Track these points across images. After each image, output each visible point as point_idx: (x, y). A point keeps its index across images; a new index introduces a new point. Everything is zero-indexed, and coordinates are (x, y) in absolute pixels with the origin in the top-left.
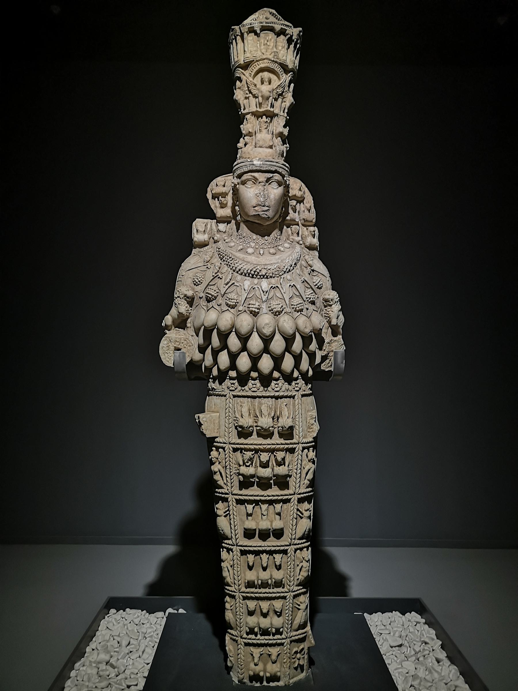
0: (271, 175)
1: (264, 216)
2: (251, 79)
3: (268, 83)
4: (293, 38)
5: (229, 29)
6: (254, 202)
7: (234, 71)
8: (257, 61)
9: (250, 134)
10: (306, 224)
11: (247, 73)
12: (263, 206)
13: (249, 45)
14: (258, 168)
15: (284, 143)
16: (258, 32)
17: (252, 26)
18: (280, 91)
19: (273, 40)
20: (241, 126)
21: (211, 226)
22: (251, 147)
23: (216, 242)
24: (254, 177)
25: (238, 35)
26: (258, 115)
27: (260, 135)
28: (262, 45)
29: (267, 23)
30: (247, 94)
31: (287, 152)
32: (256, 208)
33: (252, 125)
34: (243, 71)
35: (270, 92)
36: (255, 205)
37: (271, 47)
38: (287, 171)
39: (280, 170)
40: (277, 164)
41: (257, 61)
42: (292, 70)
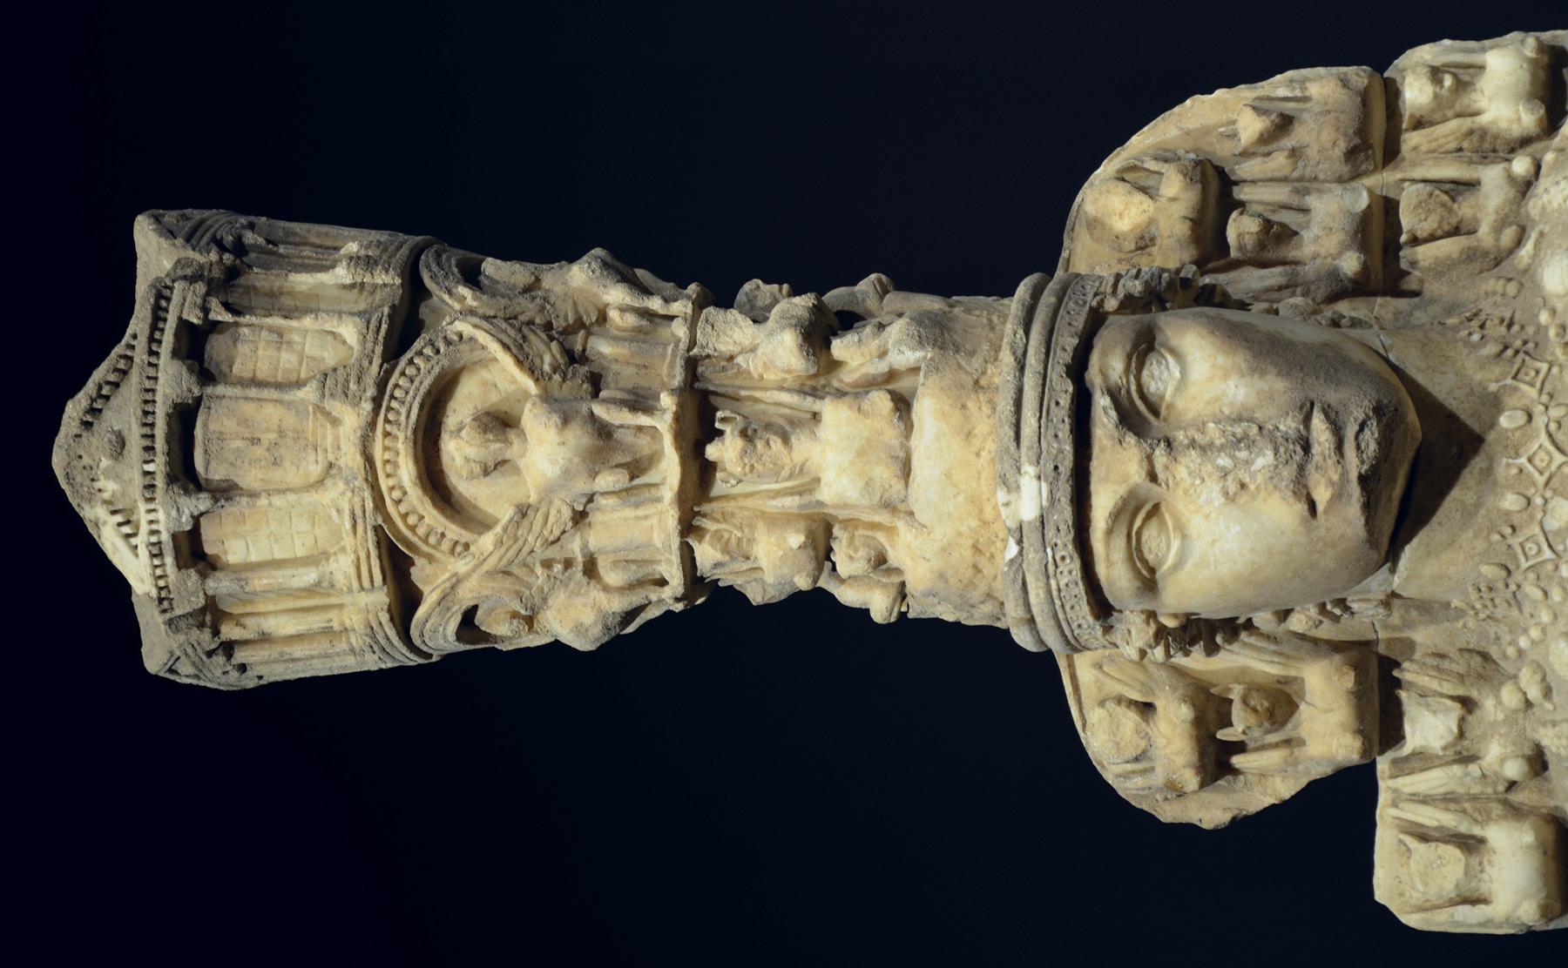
0: (1101, 402)
1: (1371, 439)
2: (487, 541)
5: (164, 687)
6: (1281, 512)
10: (1377, 135)
12: (1307, 448)
19: (248, 408)
21: (1424, 800)
23: (1538, 762)
24: (1116, 516)
27: (828, 476)
28: (276, 475)
32: (1322, 496)
35: (566, 421)
36: (1301, 507)
37: (290, 420)
39: (1067, 342)
40: (1033, 361)
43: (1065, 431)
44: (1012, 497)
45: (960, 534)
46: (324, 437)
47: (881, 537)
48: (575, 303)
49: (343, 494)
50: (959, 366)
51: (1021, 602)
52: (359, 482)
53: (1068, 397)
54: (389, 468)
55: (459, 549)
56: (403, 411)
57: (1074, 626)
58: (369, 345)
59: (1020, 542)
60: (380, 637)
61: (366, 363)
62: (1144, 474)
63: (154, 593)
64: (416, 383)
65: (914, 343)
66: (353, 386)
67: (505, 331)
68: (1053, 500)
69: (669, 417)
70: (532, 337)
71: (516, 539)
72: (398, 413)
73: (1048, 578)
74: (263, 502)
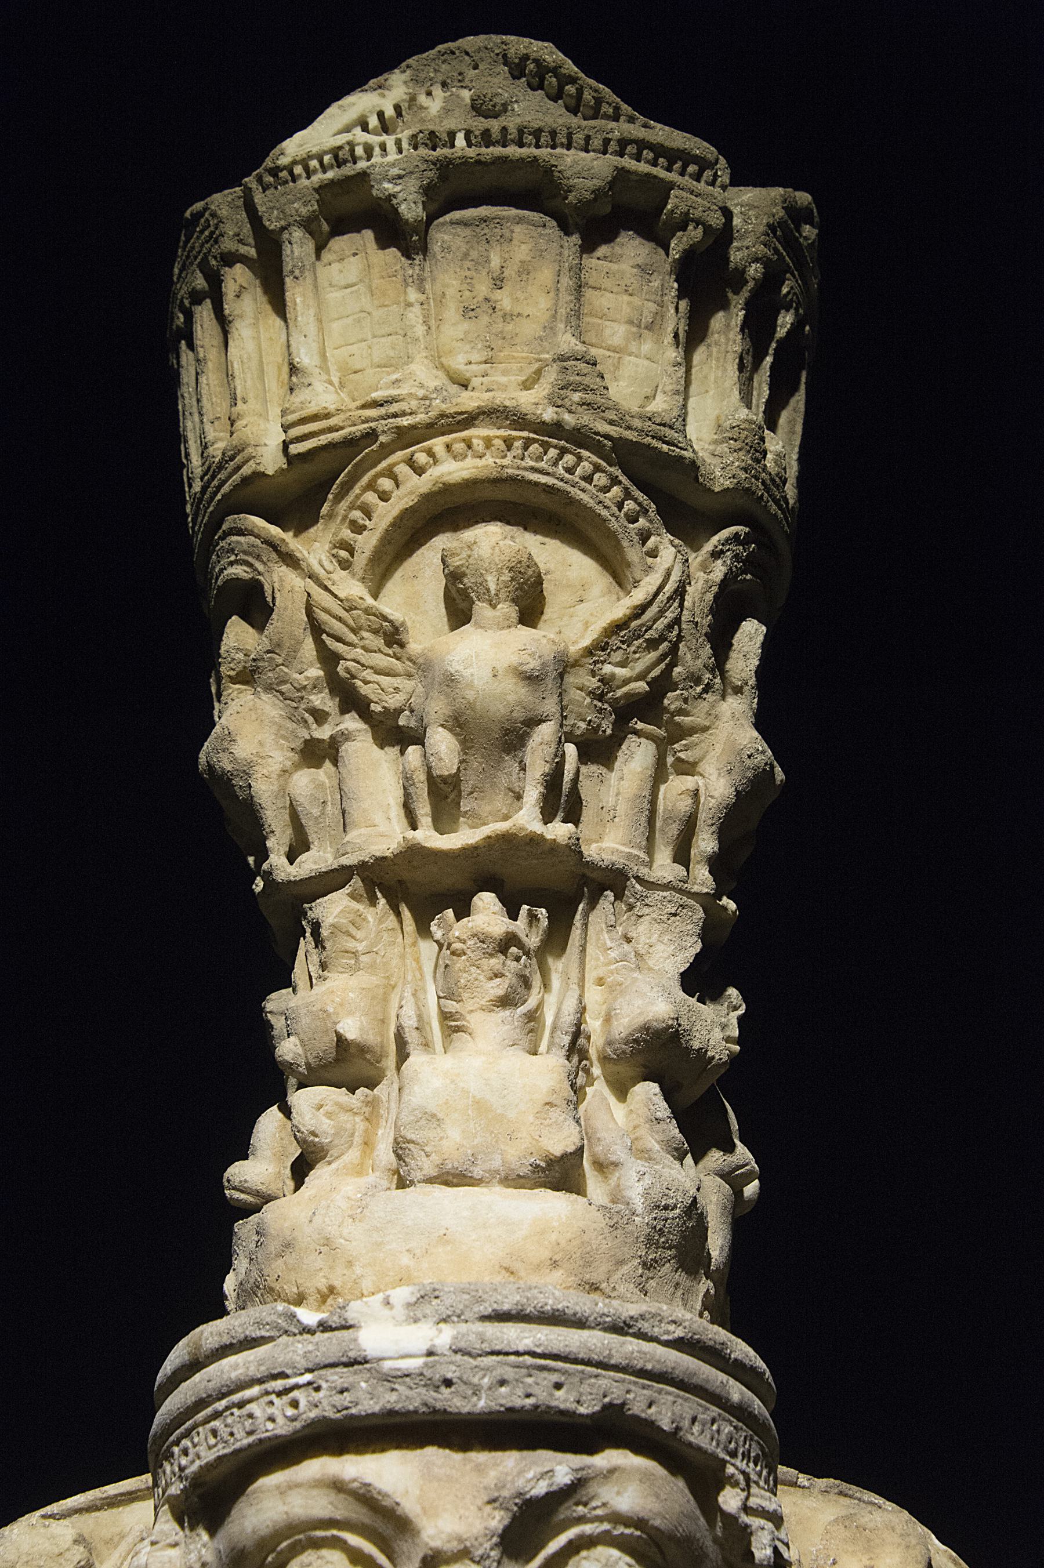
0: (561, 1468)
3: (507, 609)
4: (736, 256)
7: (209, 545)
8: (408, 437)
9: (348, 1066)
11: (315, 548)
13: (336, 326)
14: (408, 1398)
15: (698, 1133)
16: (411, 209)
17: (348, 170)
18: (630, 673)
19: (545, 274)
20: (276, 1002)
22: (351, 1187)
24: (366, 1498)
25: (230, 259)
26: (418, 889)
28: (452, 312)
29: (486, 138)
30: (320, 717)
31: (744, 1221)
33: (364, 979)
34: (275, 531)
35: (531, 679)
37: (529, 329)
38: (740, 1412)
39: (666, 1410)
40: (629, 1348)
41: (407, 437)
42: (738, 507)
43: (511, 1397)
44: (399, 1311)
45: (350, 1264)
46: (505, 373)
47: (352, 1155)
48: (705, 729)
49: (422, 386)
50: (621, 1262)
51: (226, 1340)
52: (439, 405)
53: (570, 1405)
54: (459, 447)
55: (343, 554)
56: (542, 465)
57: (186, 1443)
58: (637, 423)
59: (324, 1327)
60: (222, 476)
61: (611, 415)
62: (436, 1544)
63: (284, 161)
64: (583, 484)
65: (656, 1194)
66: (576, 397)
67: (662, 613)
68: (391, 1379)
69: (536, 826)
70: (653, 655)
71: (354, 631)
72: (539, 459)
73: (260, 1381)
74: (413, 295)
